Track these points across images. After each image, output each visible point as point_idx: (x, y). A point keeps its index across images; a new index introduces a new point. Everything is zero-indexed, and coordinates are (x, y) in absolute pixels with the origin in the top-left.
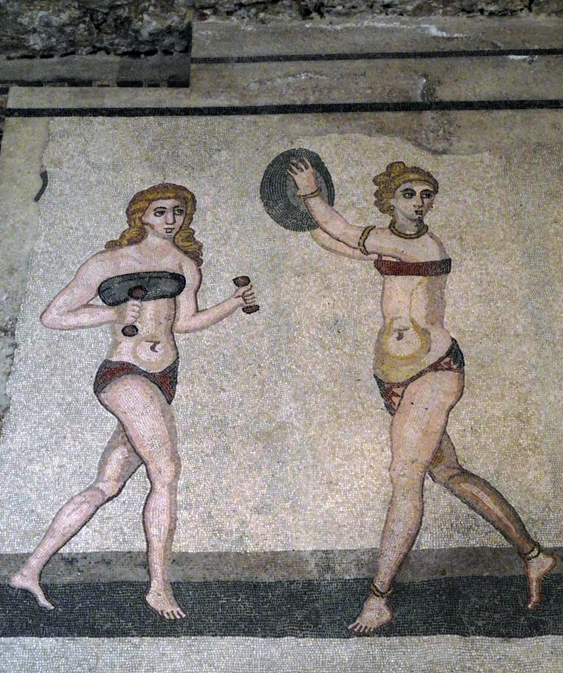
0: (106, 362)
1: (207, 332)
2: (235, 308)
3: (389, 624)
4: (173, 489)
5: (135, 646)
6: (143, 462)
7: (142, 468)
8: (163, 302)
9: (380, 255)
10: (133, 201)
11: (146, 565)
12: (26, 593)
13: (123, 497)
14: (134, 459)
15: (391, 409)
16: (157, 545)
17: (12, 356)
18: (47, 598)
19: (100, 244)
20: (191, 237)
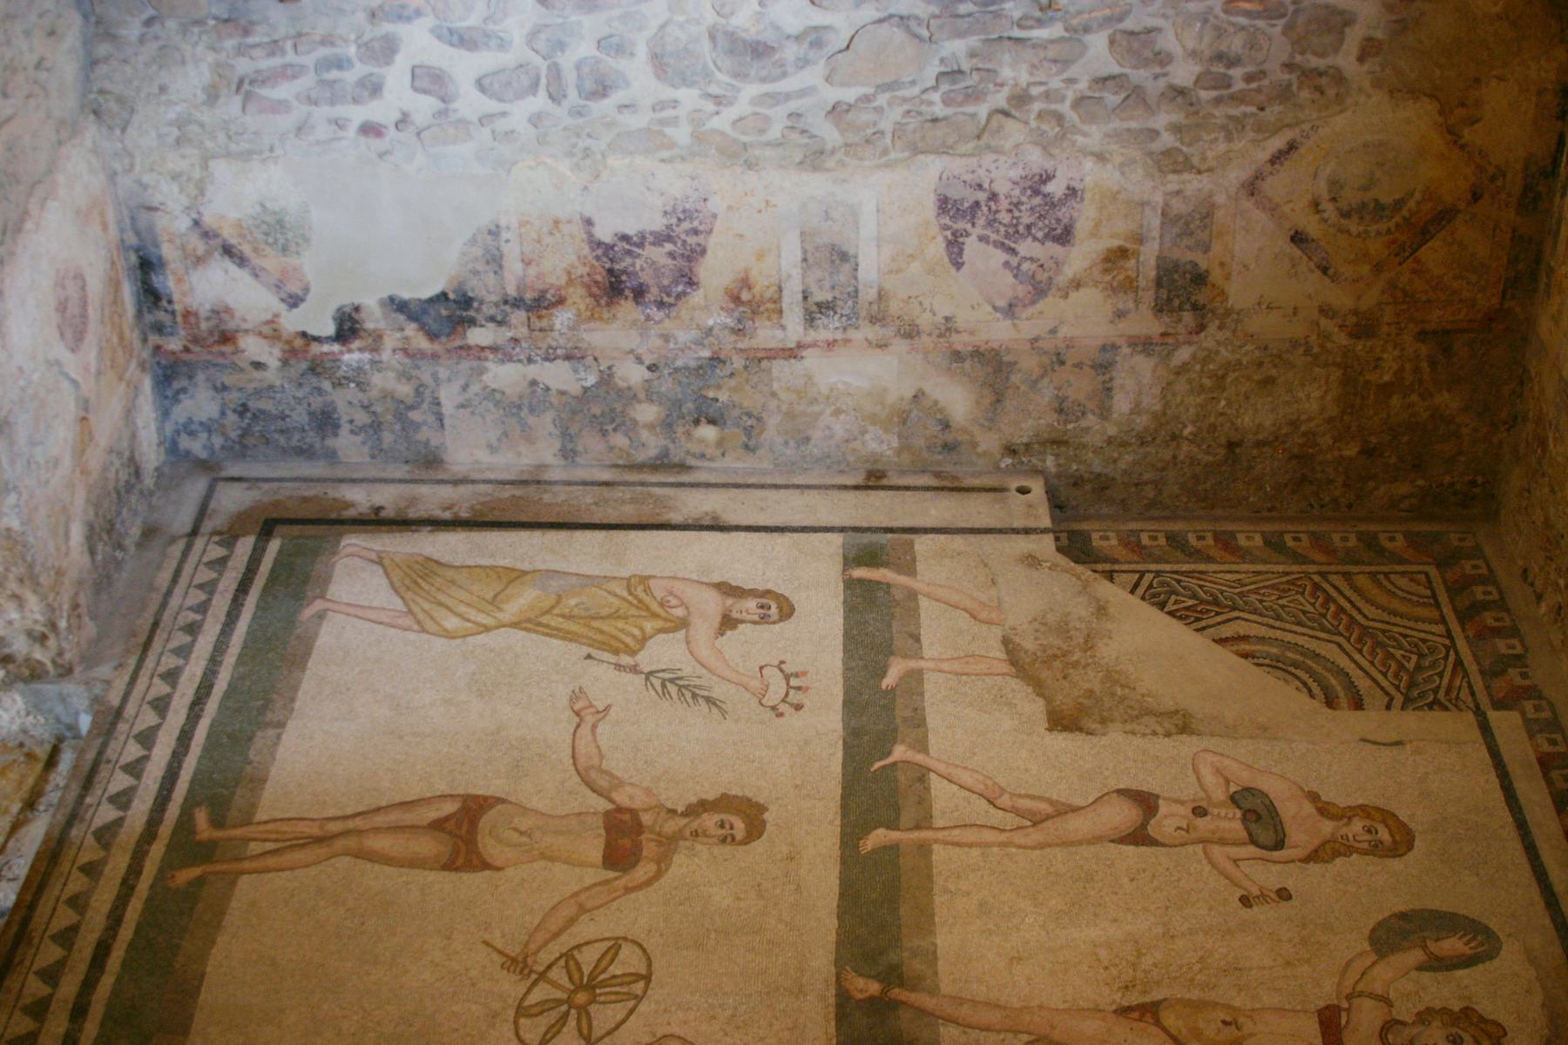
0: (1157, 797)
1: (1208, 868)
2: (1245, 889)
3: (850, 998)
4: (1003, 845)
5: (831, 823)
6: (1035, 824)
7: (1029, 823)
8: (1244, 834)
9: (1348, 1010)
10: (1378, 809)
11: (918, 827)
12: (889, 753)
13: (992, 810)
14: (1038, 818)
15: (1124, 1011)
16: (940, 835)
17: (1155, 733)
18: (884, 767)
19: (1314, 786)
20: (1336, 854)
